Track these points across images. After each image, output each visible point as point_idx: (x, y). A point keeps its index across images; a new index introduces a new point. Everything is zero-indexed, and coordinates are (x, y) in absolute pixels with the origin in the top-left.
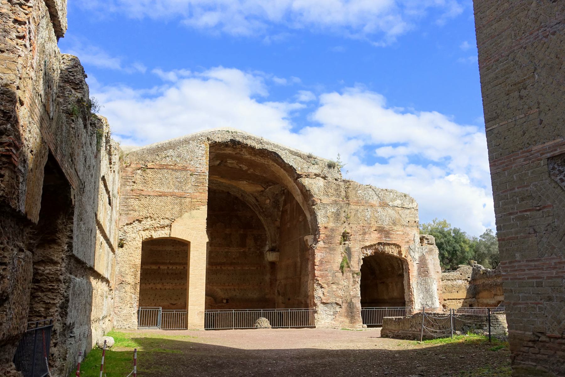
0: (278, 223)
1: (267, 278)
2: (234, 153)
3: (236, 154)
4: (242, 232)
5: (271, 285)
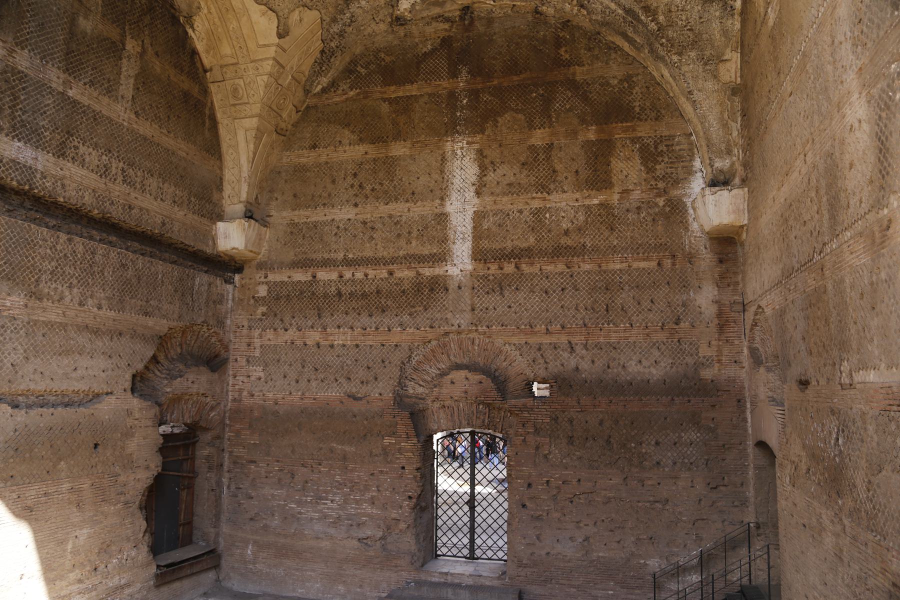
0: (731, 70)
1: (705, 298)
4: (592, 136)
5: (721, 328)
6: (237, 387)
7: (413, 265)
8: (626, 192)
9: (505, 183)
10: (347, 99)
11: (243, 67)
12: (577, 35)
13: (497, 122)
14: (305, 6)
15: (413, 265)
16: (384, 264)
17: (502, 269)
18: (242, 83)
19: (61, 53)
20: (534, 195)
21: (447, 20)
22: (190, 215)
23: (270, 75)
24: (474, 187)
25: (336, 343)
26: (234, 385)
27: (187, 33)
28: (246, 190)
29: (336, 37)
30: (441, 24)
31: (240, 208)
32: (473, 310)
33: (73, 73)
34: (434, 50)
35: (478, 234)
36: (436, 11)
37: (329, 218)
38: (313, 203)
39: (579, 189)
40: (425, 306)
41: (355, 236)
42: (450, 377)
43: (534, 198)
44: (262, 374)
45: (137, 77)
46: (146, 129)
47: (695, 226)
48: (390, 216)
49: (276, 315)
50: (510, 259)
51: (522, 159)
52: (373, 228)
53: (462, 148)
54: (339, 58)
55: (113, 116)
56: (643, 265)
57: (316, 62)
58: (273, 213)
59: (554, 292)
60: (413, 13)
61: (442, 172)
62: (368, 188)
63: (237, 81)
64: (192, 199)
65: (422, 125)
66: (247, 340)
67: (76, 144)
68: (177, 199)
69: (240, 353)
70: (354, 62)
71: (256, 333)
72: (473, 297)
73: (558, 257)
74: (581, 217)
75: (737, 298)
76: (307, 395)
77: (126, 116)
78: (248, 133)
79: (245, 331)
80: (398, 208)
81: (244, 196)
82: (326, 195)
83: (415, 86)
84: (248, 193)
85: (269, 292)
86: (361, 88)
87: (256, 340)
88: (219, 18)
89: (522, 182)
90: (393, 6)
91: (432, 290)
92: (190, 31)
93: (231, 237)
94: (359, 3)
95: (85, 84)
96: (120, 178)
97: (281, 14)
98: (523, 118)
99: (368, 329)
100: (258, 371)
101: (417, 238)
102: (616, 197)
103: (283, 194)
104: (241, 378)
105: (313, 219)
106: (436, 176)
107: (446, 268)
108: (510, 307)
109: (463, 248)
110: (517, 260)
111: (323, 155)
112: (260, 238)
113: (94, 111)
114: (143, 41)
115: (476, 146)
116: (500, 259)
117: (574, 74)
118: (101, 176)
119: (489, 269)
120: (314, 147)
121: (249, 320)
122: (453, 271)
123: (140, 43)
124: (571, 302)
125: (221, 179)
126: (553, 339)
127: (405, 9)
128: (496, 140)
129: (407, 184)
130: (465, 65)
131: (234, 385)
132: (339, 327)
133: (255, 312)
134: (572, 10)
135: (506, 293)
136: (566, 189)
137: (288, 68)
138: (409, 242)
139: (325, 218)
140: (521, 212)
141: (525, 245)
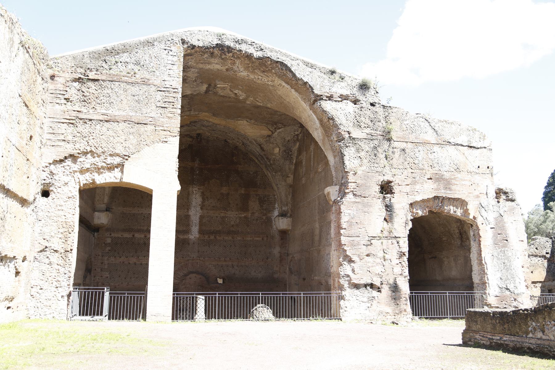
0: (290, 180)
1: (276, 251)
2: (224, 68)
3: (227, 70)
4: (243, 192)
5: (281, 261)
8: (253, 213)
21: (191, 137)
35: (201, 224)
37: (141, 212)
44: (108, 276)
47: (274, 227)
56: (257, 239)
58: (114, 207)
61: (188, 199)
75: (286, 252)
79: (100, 257)
85: (112, 241)
91: (183, 244)
102: (250, 215)
115: (201, 190)
122: (191, 237)
131: (94, 280)
140: (217, 217)
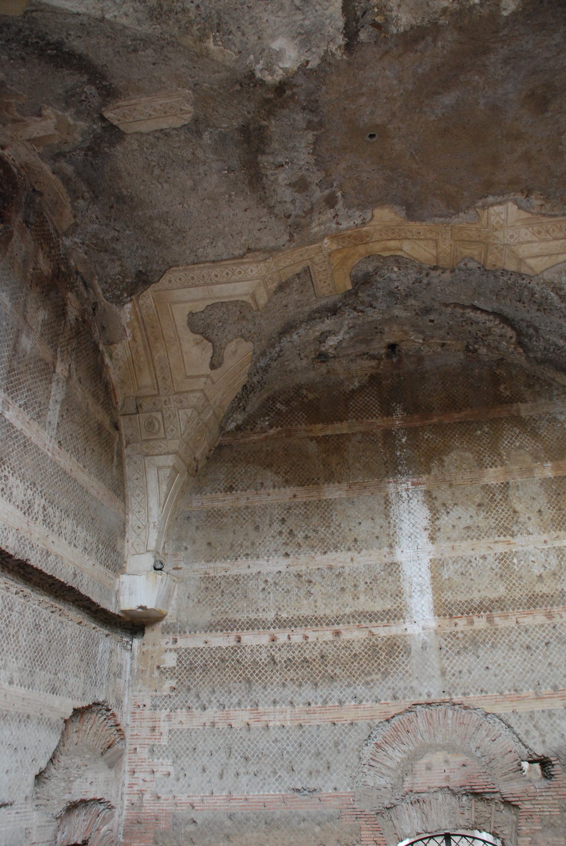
6: (136, 788)
7: (364, 625)
9: (462, 526)
10: (267, 438)
11: (163, 399)
12: (514, 372)
13: (443, 461)
14: (242, 336)
15: (364, 625)
16: (327, 625)
17: (471, 623)
18: (159, 416)
19: (4, 371)
20: (497, 539)
21: (373, 357)
22: (98, 565)
23: (195, 408)
24: (427, 533)
25: (271, 724)
26: (131, 786)
27: (103, 361)
28: (155, 537)
29: (260, 371)
30: (367, 361)
31: (148, 561)
32: (443, 673)
33: (12, 393)
34: (362, 388)
35: (438, 585)
36: (362, 348)
37: (254, 570)
38: (233, 553)
39: (545, 529)
40: (383, 673)
41: (288, 591)
42: (424, 761)
43: (496, 542)
44: (171, 769)
45: (63, 401)
46: (67, 461)
48: (330, 568)
49: (189, 689)
50: (479, 612)
51: (477, 500)
52: (310, 582)
53: (407, 490)
54: (257, 394)
55: (40, 444)
57: (236, 397)
59: (537, 648)
60: (338, 349)
61: (387, 516)
62: (301, 535)
63: (154, 414)
64: (100, 546)
65: (358, 465)
66: (151, 724)
67: (7, 474)
68: (87, 545)
69: (140, 741)
70: (272, 399)
71: (163, 714)
72: (442, 659)
73: (535, 607)
74: (554, 561)
76: (235, 795)
77: (51, 445)
78: (161, 473)
79: (147, 713)
80: (339, 558)
81: (152, 545)
82: (249, 544)
83: (345, 424)
84: (157, 541)
85: (179, 661)
86: (282, 426)
87: (162, 723)
88: (145, 348)
89: (480, 525)
90: (320, 342)
92: (107, 360)
93: (137, 591)
94: (291, 337)
95: (20, 406)
96: (41, 518)
97: (218, 344)
98: (471, 456)
99: (313, 705)
100: (165, 765)
101: (365, 592)
103: (194, 542)
104: (142, 776)
105: (234, 571)
106: (380, 521)
107: (404, 626)
108: (487, 668)
109: (423, 602)
110: (488, 613)
111: (242, 499)
112: (169, 595)
113: (25, 437)
114: (70, 366)
115: (424, 487)
116: (468, 613)
117: (518, 411)
118: (25, 513)
119: (456, 624)
120: (231, 489)
121: (153, 698)
123: (68, 367)
124: (559, 659)
125: (125, 524)
126: (546, 705)
127: (331, 346)
128: (444, 480)
129: (347, 530)
130: (399, 403)
132: (275, 702)
133: (161, 687)
134: (507, 349)
135: (481, 653)
136: (531, 531)
137: (212, 402)
138: (356, 597)
139: (248, 571)
140: (484, 558)
141: (494, 595)
